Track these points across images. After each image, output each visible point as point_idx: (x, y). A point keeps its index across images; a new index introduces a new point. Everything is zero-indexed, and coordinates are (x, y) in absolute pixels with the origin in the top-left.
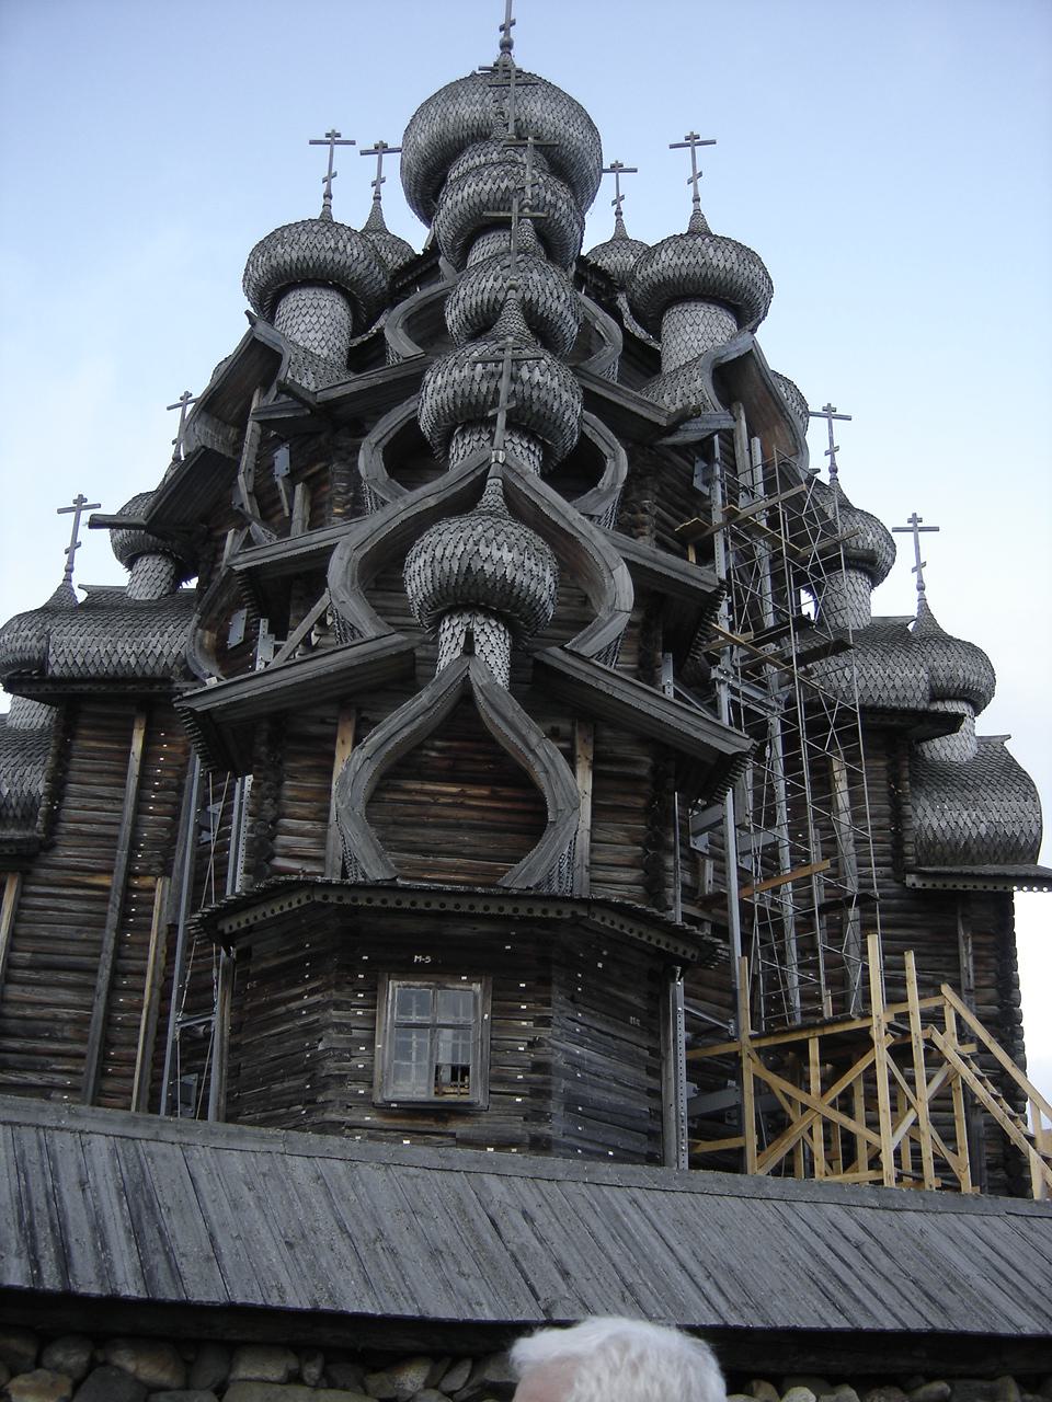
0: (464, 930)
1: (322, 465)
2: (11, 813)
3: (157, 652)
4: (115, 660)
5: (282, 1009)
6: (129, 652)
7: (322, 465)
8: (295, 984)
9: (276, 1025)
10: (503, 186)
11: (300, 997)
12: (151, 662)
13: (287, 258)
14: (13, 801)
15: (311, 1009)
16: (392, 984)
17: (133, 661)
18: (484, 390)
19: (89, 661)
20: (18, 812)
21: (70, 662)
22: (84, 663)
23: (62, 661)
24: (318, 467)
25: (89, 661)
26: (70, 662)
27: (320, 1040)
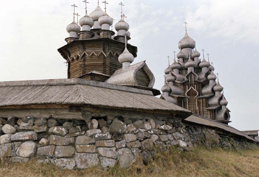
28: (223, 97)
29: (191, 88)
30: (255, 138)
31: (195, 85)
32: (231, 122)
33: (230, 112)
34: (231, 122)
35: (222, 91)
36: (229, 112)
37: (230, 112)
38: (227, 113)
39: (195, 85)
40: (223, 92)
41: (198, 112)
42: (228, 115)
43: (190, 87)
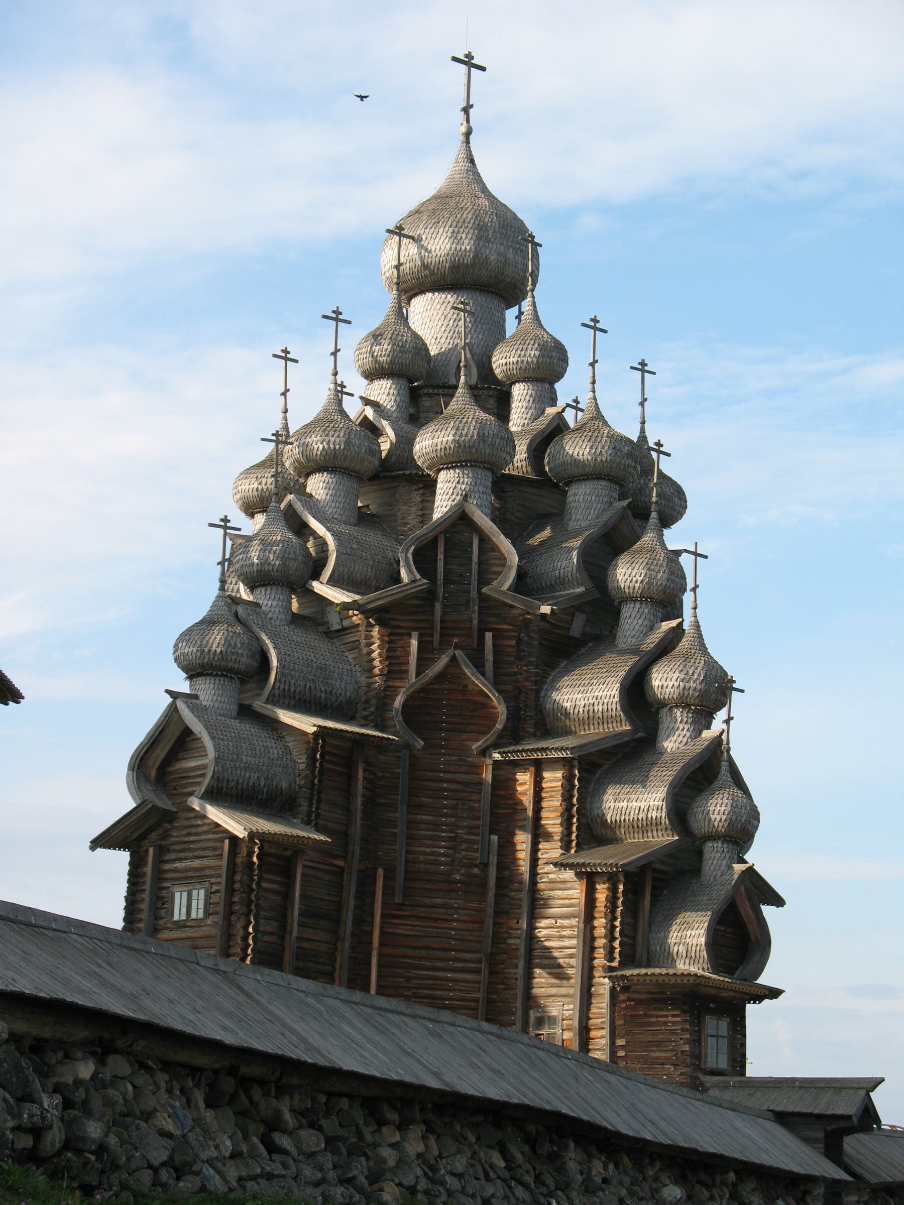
0: (724, 994)
1: (509, 627)
2: (260, 797)
3: (338, 692)
4: (313, 694)
5: (654, 1020)
6: (323, 689)
7: (509, 627)
8: (661, 1010)
9: (650, 1026)
10: (627, 462)
11: (666, 1016)
12: (333, 699)
13: (483, 452)
14: (265, 790)
15: (674, 1023)
16: (707, 1017)
17: (323, 695)
18: (712, 698)
19: (298, 691)
20: (264, 796)
21: (287, 688)
22: (295, 691)
23: (282, 687)
24: (504, 627)
25: (298, 691)
26: (287, 688)
27: (681, 1039)
28: (724, 765)
29: (444, 660)
30: (852, 1144)
31: (489, 636)
32: (775, 993)
33: (778, 902)
34: (775, 993)
35: (721, 715)
36: (768, 911)
37: (778, 902)
38: (745, 909)
39: (489, 636)
40: (727, 722)
41: (492, 881)
42: (752, 929)
43: (442, 650)
